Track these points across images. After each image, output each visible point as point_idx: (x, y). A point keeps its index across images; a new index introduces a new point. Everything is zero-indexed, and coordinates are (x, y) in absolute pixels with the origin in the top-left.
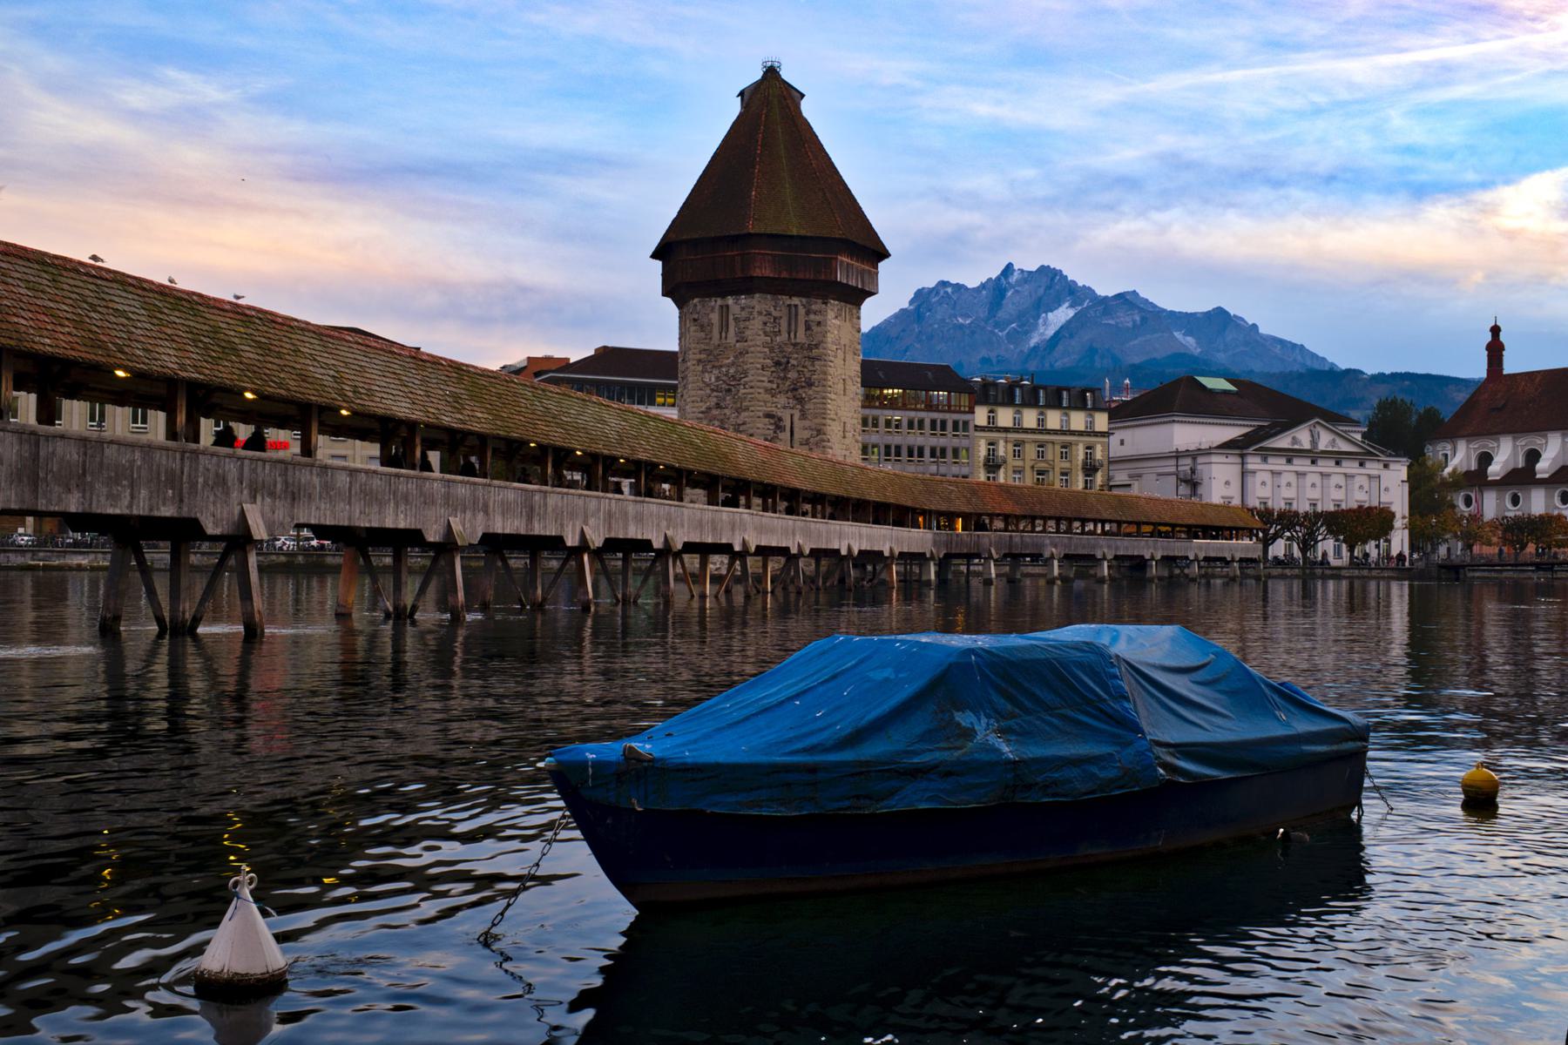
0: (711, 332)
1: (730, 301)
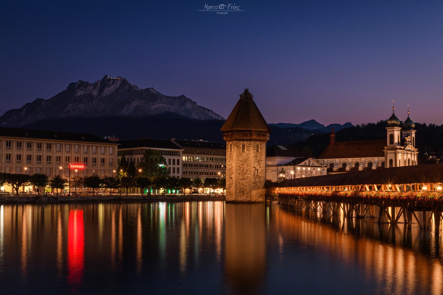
0: (240, 149)
1: (245, 142)
